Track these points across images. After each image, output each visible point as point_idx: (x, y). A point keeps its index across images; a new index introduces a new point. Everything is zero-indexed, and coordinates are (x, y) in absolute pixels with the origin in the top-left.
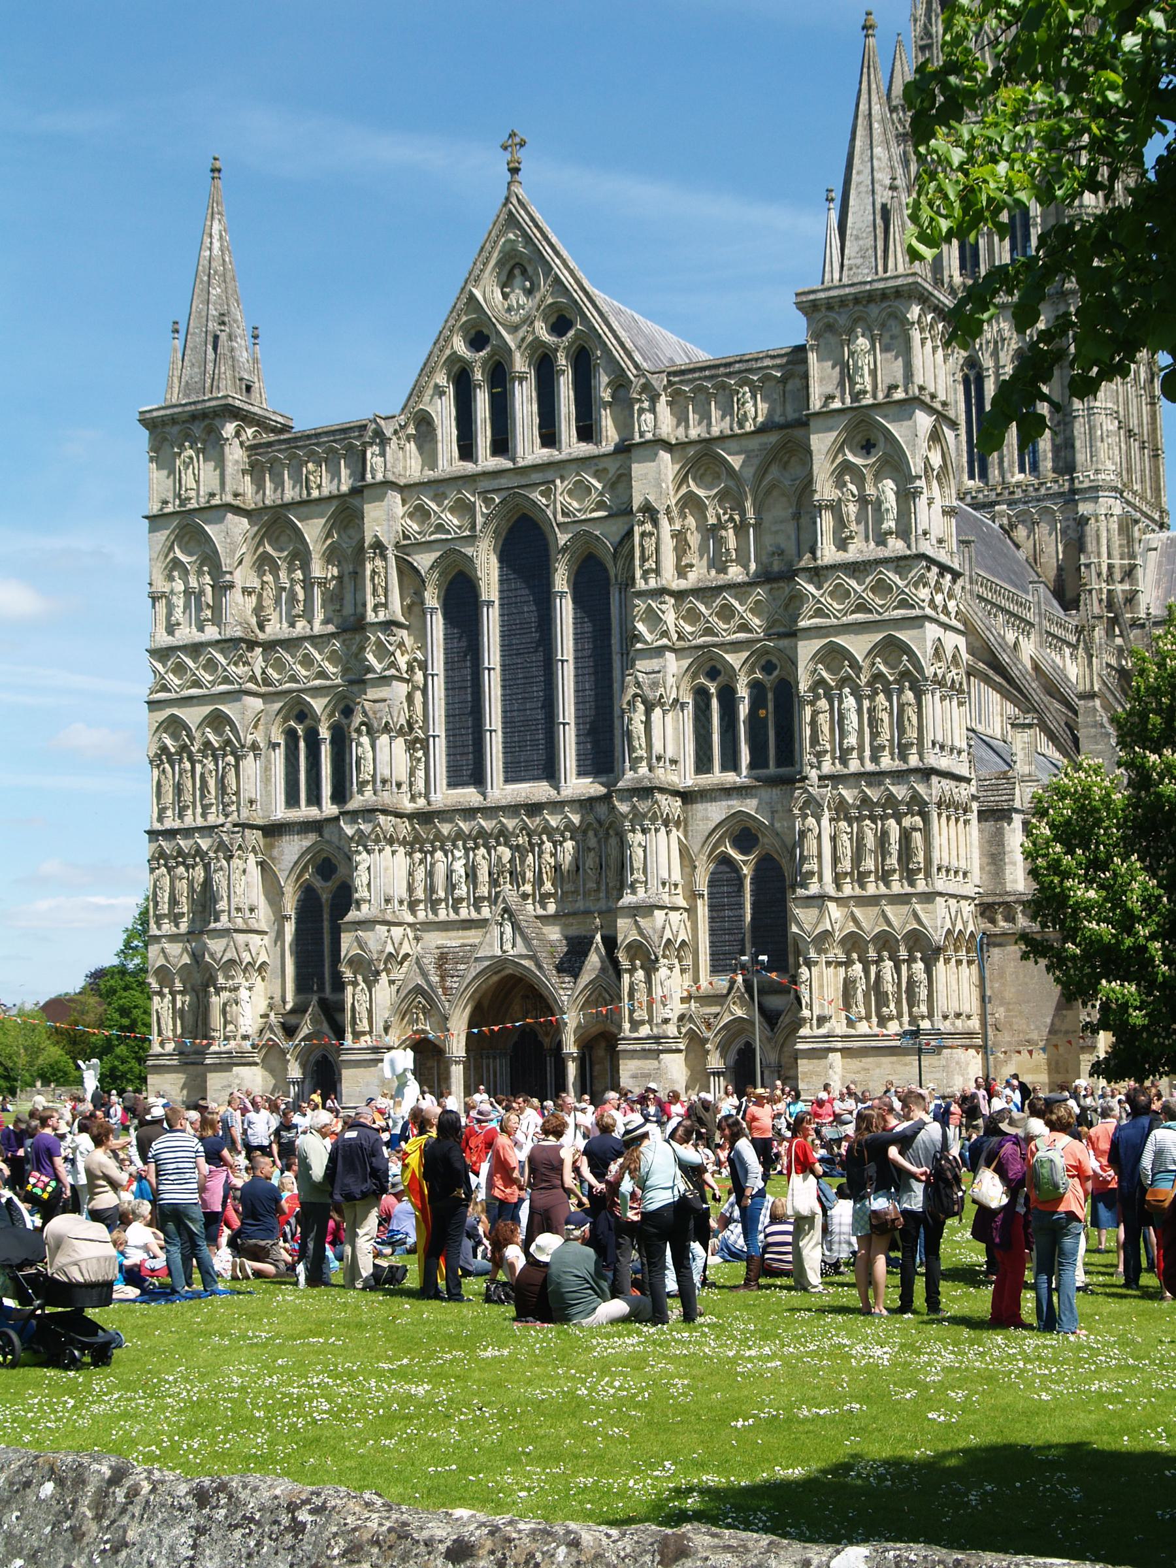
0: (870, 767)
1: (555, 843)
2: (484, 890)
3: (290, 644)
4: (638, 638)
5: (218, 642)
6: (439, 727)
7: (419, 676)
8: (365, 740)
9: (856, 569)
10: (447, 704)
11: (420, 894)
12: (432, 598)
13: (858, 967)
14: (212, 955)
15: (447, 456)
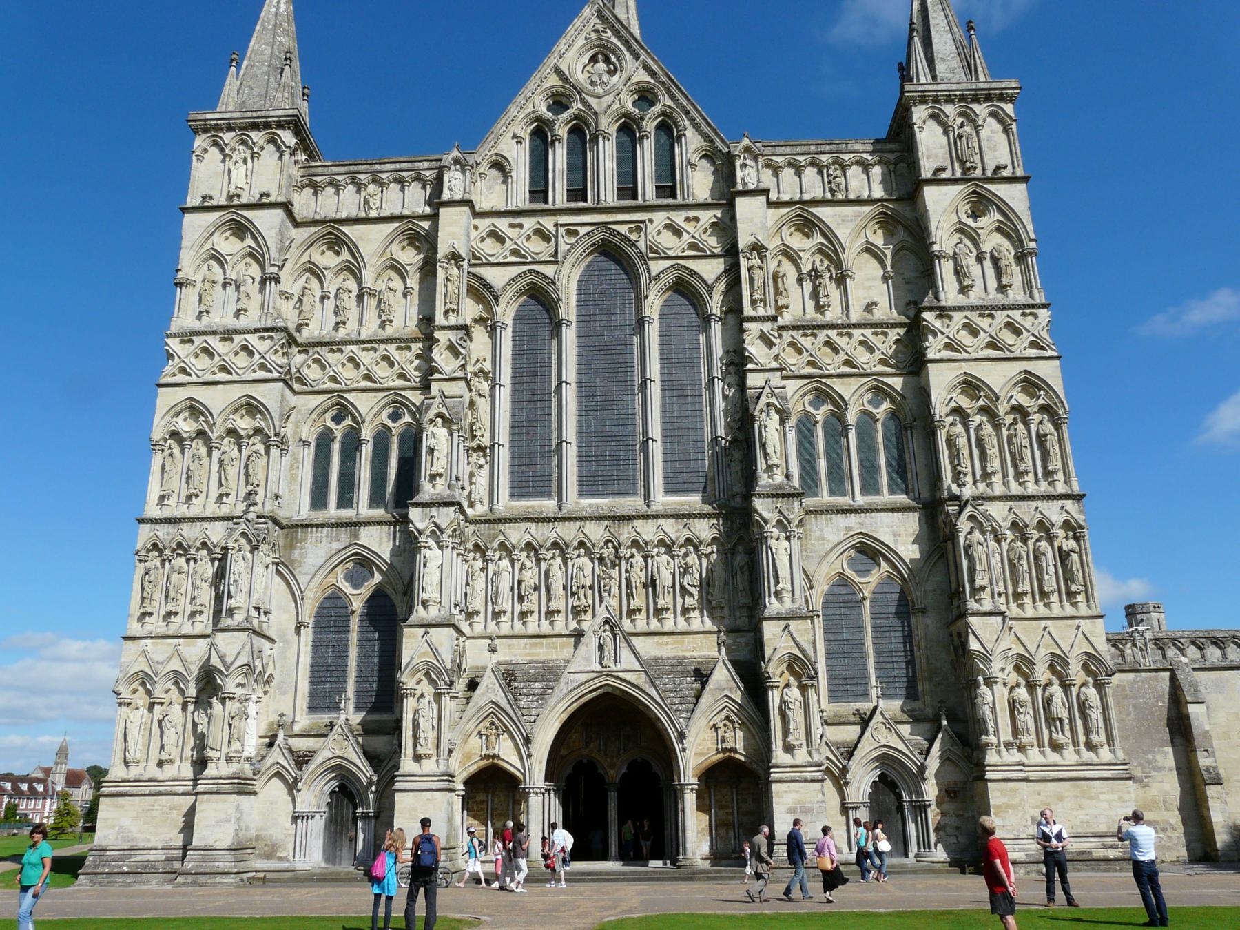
0: (1015, 489)
1: (645, 558)
2: (558, 603)
3: (334, 345)
4: (749, 359)
5: (256, 330)
6: (504, 437)
7: (485, 386)
8: (441, 432)
9: (985, 310)
10: (513, 416)
11: (477, 603)
12: (506, 312)
13: (1022, 693)
14: (222, 658)
15: (520, 197)
